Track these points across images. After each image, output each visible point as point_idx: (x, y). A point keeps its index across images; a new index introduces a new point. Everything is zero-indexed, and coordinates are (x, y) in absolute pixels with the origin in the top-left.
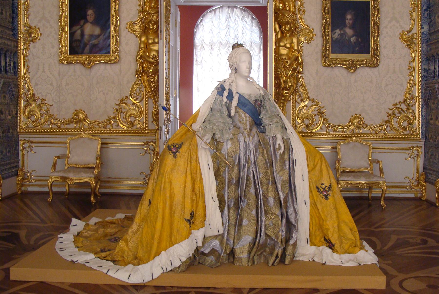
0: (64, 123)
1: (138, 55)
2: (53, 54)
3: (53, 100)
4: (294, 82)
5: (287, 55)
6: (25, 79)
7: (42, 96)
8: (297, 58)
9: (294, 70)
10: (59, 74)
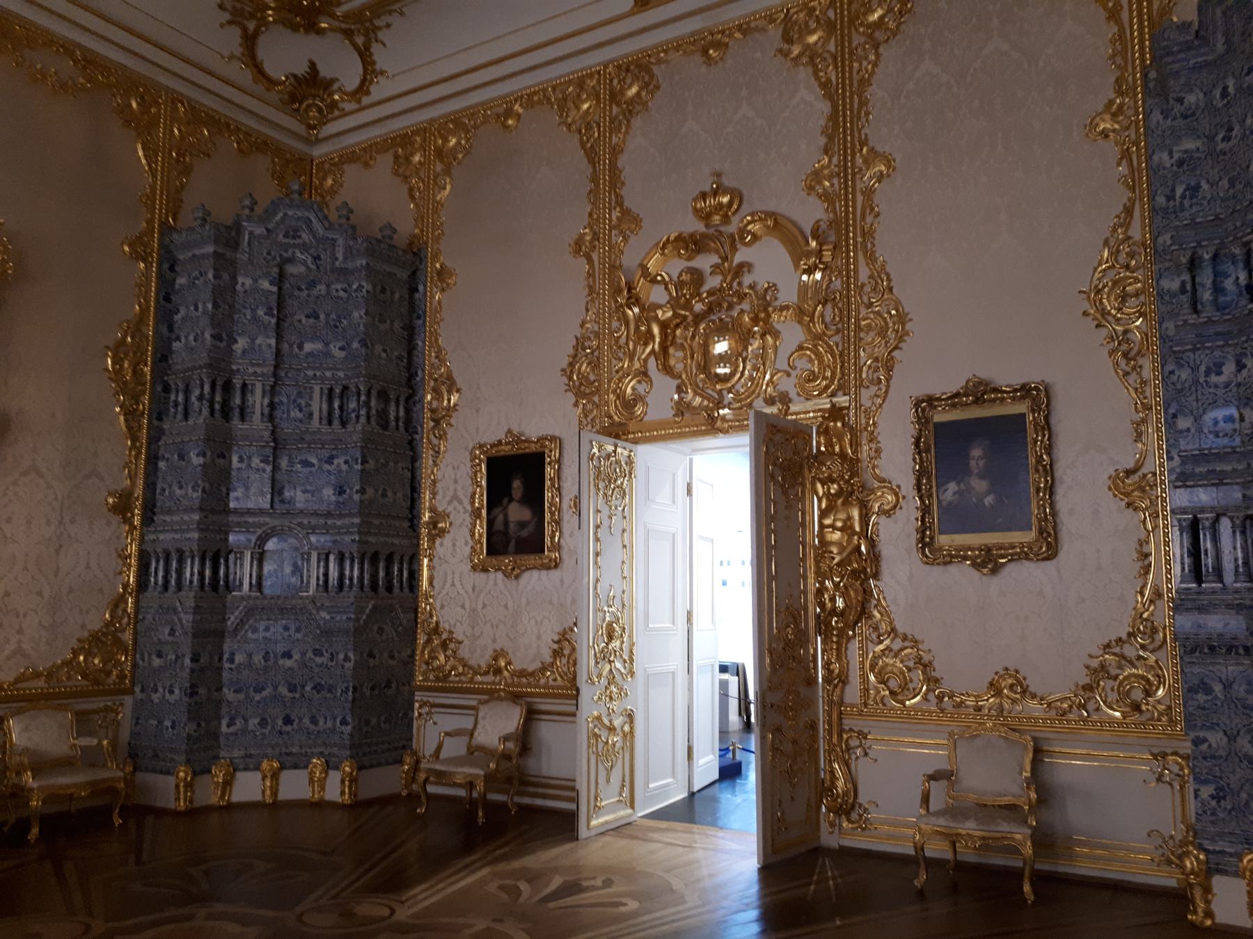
0: (476, 673)
5: (838, 544)
10: (474, 589)
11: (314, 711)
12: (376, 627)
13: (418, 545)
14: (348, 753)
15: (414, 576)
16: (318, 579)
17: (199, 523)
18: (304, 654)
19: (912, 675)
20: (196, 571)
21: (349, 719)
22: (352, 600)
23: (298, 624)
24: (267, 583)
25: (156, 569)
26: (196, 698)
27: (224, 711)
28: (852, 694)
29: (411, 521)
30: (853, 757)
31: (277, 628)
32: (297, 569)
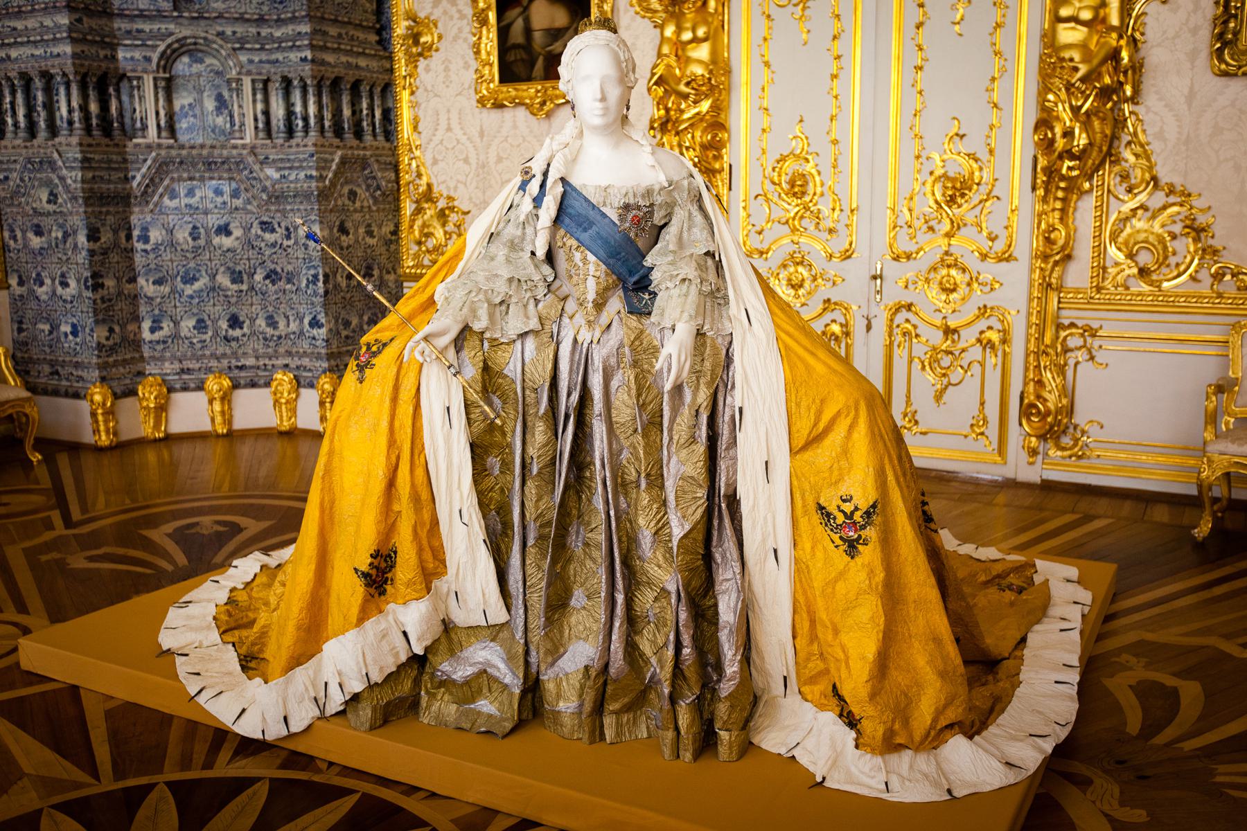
1: (653, 75)
2: (466, 86)
3: (470, 199)
4: (1103, 132)
5: (1083, 46)
6: (410, 150)
7: (448, 188)
8: (1115, 55)
9: (1105, 93)
11: (271, 309)
12: (346, 190)
13: (391, 71)
14: (325, 365)
15: (389, 117)
16: (256, 120)
17: (71, 29)
18: (247, 229)
19: (1178, 245)
20: (75, 104)
21: (322, 318)
22: (311, 149)
23: (234, 185)
24: (182, 125)
25: (13, 104)
26: (101, 292)
27: (143, 310)
28: (1078, 275)
29: (379, 32)
30: (1071, 362)
31: (205, 193)
32: (222, 104)
